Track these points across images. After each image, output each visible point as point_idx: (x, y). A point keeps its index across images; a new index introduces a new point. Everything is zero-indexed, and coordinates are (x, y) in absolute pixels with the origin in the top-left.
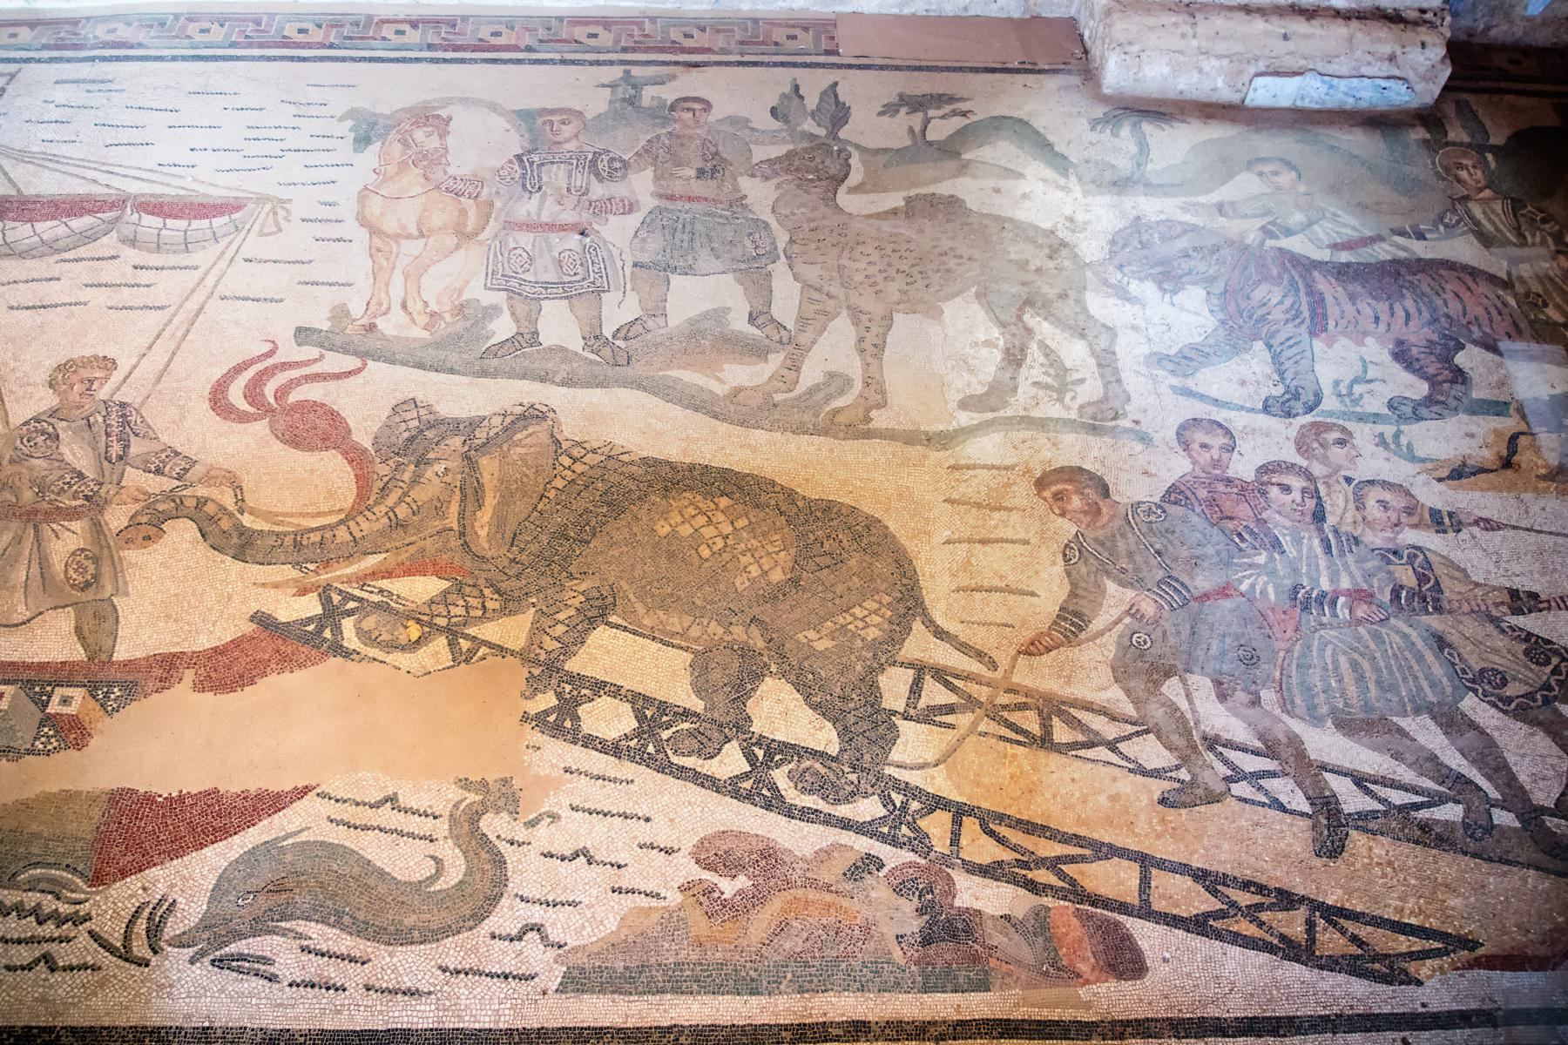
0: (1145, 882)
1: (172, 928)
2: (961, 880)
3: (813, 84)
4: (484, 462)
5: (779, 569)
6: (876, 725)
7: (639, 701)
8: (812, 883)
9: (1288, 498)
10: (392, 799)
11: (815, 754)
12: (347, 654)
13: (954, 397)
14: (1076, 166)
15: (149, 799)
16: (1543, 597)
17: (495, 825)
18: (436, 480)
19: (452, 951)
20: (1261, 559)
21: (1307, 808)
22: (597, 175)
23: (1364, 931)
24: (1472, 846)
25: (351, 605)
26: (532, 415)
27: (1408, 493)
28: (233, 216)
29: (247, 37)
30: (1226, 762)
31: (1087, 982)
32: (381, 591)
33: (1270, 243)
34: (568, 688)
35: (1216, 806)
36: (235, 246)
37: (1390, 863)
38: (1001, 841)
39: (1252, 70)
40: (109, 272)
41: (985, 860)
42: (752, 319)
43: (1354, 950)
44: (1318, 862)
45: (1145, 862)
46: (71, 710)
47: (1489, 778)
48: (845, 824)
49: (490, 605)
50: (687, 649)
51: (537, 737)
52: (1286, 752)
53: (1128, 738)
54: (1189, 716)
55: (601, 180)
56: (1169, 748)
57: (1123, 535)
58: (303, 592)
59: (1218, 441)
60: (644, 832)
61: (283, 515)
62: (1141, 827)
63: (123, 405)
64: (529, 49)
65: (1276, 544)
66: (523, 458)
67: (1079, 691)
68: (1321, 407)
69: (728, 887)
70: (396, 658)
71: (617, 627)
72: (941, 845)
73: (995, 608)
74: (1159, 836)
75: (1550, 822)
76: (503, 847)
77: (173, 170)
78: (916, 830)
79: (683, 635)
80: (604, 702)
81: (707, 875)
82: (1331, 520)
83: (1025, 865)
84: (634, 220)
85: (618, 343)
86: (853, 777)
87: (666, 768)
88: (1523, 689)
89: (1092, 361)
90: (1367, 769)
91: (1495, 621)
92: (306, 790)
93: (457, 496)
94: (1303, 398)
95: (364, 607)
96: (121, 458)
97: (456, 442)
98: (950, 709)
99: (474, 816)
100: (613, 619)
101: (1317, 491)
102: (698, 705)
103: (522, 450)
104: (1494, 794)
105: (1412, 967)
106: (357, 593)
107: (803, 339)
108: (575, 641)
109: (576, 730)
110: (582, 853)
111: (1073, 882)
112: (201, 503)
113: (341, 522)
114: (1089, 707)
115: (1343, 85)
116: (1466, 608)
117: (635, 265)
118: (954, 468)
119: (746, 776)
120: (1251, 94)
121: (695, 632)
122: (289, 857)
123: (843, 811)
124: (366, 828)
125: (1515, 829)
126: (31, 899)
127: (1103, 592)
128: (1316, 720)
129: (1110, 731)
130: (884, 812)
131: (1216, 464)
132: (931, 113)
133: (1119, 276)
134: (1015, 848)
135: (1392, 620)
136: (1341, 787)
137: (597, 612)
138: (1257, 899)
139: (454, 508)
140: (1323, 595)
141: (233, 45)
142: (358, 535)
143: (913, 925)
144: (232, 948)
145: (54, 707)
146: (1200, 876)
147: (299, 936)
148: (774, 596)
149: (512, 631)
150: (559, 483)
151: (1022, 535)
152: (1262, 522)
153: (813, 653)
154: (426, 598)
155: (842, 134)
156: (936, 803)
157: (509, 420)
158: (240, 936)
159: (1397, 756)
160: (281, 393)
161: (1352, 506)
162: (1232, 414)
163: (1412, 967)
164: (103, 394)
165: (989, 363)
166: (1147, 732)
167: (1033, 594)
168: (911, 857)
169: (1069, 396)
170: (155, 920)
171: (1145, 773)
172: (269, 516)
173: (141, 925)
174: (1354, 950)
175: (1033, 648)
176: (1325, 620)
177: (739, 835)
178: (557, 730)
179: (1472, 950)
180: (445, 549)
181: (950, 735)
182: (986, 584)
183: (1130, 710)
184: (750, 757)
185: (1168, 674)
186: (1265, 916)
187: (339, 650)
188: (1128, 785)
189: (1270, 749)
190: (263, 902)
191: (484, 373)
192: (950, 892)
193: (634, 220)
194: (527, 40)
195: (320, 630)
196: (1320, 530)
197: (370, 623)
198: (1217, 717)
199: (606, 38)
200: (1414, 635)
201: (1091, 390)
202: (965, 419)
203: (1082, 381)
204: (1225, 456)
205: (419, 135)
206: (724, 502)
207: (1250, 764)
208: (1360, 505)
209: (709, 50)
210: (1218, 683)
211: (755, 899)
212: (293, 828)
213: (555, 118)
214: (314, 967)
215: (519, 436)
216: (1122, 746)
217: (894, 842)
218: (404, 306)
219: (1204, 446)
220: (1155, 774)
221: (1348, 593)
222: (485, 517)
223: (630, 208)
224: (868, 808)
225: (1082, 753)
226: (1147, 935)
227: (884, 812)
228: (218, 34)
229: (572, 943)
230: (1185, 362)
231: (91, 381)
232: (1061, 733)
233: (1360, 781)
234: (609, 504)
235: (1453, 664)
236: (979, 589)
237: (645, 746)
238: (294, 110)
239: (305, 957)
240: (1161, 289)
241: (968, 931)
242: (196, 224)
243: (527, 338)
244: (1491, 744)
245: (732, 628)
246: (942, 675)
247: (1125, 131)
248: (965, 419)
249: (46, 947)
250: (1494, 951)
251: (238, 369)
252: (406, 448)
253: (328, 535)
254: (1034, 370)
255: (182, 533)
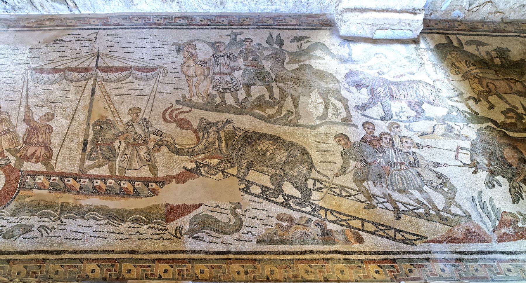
0: (363, 224)
1: (183, 232)
2: (328, 223)
3: (275, 33)
4: (220, 132)
5: (284, 157)
6: (308, 192)
7: (260, 186)
8: (300, 224)
9: (387, 141)
10: (218, 206)
11: (297, 198)
12: (203, 176)
13: (315, 117)
14: (336, 56)
15: (173, 205)
16: (440, 164)
17: (238, 211)
18: (212, 137)
19: (235, 236)
20: (381, 155)
21: (393, 209)
22: (231, 60)
23: (405, 235)
24: (426, 218)
25: (201, 165)
26: (228, 122)
27: (412, 139)
28: (156, 72)
29: (146, 22)
30: (377, 200)
31: (353, 244)
32: (207, 162)
33: (380, 76)
34: (247, 183)
35: (375, 209)
36: (158, 79)
37: (410, 221)
38: (334, 216)
39: (376, 28)
40: (134, 86)
41: (332, 220)
42: (270, 97)
43: (403, 238)
44: (396, 221)
45: (362, 220)
46: (153, 187)
47: (429, 203)
48: (304, 212)
49: (229, 165)
50: (268, 175)
51: (243, 194)
52: (388, 198)
53: (357, 194)
54: (369, 190)
55: (232, 61)
56: (365, 196)
57: (353, 150)
58: (192, 162)
59: (371, 127)
60: (267, 213)
61: (184, 145)
62: (361, 213)
63: (145, 119)
64: (209, 25)
65: (385, 151)
66: (228, 131)
67: (347, 184)
68: (393, 119)
69: (284, 224)
70: (212, 176)
71: (254, 170)
72: (323, 216)
73: (329, 166)
74: (365, 215)
75: (442, 213)
76: (241, 216)
77: (140, 59)
78: (318, 213)
79: (267, 172)
80: (254, 186)
81: (280, 222)
82: (396, 146)
83: (339, 221)
84: (241, 72)
85: (243, 103)
86: (305, 202)
87: (269, 200)
88: (436, 184)
89: (343, 108)
90: (405, 201)
91: (430, 169)
92: (202, 204)
93: (217, 141)
94: (389, 116)
95: (204, 166)
96: (148, 132)
97: (214, 128)
98: (321, 188)
99: (234, 210)
100: (253, 168)
101: (393, 139)
102: (273, 187)
103: (228, 130)
104: (430, 207)
105: (415, 242)
106: (202, 162)
107: (282, 102)
108: (246, 174)
109: (250, 192)
110: (256, 217)
111: (349, 224)
112: (167, 142)
113: (195, 146)
114: (348, 188)
115: (397, 32)
116: (424, 166)
117: (243, 84)
118: (317, 134)
119: (284, 202)
120: (375, 35)
121: (270, 171)
122: (202, 218)
123: (303, 209)
124: (214, 212)
125: (434, 215)
126: (156, 226)
127: (350, 163)
128: (394, 191)
129: (353, 193)
130: (311, 210)
131: (371, 132)
132: (302, 42)
133: (348, 85)
134: (337, 217)
135: (409, 169)
136: (400, 205)
137: (249, 167)
138: (384, 228)
139: (217, 143)
140: (395, 163)
141: (144, 25)
142: (199, 149)
143: (320, 232)
144: (195, 235)
145: (150, 187)
146: (373, 223)
147: (207, 233)
148: (285, 163)
149: (233, 171)
150: (237, 138)
151: (333, 150)
152: (381, 146)
153: (293, 176)
154: (216, 163)
155: (283, 48)
156: (322, 208)
157: (224, 123)
158: (196, 233)
159: (410, 198)
160: (177, 116)
161: (400, 142)
162: (374, 120)
163: (415, 242)
164: (140, 116)
165: (321, 108)
166: (361, 193)
167: (336, 163)
168: (318, 219)
169: (339, 116)
170: (180, 229)
171: (360, 201)
172: (181, 145)
173: (178, 231)
174: (403, 238)
175: (336, 175)
176: (395, 169)
177: (285, 214)
178: (246, 192)
179: (426, 239)
180: (217, 152)
181: (323, 194)
182: (326, 161)
183: (357, 189)
184: (284, 198)
185: (364, 180)
186: (386, 231)
187: (201, 174)
188: (358, 204)
189: (385, 197)
190: (199, 226)
191: (216, 111)
192: (326, 226)
193: (241, 72)
194: (209, 23)
195: (197, 170)
196: (394, 149)
197: (206, 169)
198: (374, 190)
199: (226, 22)
200: (414, 173)
201: (344, 115)
202: (318, 122)
203: (341, 113)
204: (373, 131)
205: (190, 49)
206: (271, 142)
207: (382, 200)
208: (402, 142)
209: (249, 25)
210: (374, 183)
211: (290, 227)
212: (201, 212)
213: (219, 44)
214: (211, 239)
215: (227, 126)
216: (356, 196)
217: (314, 216)
218: (196, 94)
219: (368, 128)
220: (363, 202)
221: (400, 163)
222: (223, 145)
223: (240, 69)
224: (308, 209)
225: (348, 198)
226: (363, 235)
227: (311, 210)
228: (140, 22)
229: (257, 235)
230: (363, 107)
231: (137, 113)
232: (344, 194)
233: (403, 204)
234: (248, 142)
235: (422, 179)
236: (325, 162)
237: (264, 196)
238: (161, 43)
239: (209, 237)
240: (357, 89)
241: (330, 234)
242: (150, 73)
243: (224, 102)
244: (430, 197)
245: (277, 171)
246: (320, 181)
247: (346, 46)
248: (318, 122)
249: (162, 235)
250: (431, 239)
251: (166, 110)
252: (204, 129)
253: (193, 149)
254: (331, 110)
255: (164, 149)
